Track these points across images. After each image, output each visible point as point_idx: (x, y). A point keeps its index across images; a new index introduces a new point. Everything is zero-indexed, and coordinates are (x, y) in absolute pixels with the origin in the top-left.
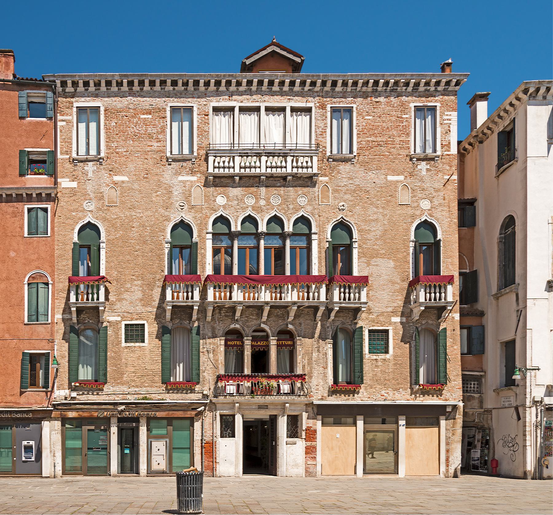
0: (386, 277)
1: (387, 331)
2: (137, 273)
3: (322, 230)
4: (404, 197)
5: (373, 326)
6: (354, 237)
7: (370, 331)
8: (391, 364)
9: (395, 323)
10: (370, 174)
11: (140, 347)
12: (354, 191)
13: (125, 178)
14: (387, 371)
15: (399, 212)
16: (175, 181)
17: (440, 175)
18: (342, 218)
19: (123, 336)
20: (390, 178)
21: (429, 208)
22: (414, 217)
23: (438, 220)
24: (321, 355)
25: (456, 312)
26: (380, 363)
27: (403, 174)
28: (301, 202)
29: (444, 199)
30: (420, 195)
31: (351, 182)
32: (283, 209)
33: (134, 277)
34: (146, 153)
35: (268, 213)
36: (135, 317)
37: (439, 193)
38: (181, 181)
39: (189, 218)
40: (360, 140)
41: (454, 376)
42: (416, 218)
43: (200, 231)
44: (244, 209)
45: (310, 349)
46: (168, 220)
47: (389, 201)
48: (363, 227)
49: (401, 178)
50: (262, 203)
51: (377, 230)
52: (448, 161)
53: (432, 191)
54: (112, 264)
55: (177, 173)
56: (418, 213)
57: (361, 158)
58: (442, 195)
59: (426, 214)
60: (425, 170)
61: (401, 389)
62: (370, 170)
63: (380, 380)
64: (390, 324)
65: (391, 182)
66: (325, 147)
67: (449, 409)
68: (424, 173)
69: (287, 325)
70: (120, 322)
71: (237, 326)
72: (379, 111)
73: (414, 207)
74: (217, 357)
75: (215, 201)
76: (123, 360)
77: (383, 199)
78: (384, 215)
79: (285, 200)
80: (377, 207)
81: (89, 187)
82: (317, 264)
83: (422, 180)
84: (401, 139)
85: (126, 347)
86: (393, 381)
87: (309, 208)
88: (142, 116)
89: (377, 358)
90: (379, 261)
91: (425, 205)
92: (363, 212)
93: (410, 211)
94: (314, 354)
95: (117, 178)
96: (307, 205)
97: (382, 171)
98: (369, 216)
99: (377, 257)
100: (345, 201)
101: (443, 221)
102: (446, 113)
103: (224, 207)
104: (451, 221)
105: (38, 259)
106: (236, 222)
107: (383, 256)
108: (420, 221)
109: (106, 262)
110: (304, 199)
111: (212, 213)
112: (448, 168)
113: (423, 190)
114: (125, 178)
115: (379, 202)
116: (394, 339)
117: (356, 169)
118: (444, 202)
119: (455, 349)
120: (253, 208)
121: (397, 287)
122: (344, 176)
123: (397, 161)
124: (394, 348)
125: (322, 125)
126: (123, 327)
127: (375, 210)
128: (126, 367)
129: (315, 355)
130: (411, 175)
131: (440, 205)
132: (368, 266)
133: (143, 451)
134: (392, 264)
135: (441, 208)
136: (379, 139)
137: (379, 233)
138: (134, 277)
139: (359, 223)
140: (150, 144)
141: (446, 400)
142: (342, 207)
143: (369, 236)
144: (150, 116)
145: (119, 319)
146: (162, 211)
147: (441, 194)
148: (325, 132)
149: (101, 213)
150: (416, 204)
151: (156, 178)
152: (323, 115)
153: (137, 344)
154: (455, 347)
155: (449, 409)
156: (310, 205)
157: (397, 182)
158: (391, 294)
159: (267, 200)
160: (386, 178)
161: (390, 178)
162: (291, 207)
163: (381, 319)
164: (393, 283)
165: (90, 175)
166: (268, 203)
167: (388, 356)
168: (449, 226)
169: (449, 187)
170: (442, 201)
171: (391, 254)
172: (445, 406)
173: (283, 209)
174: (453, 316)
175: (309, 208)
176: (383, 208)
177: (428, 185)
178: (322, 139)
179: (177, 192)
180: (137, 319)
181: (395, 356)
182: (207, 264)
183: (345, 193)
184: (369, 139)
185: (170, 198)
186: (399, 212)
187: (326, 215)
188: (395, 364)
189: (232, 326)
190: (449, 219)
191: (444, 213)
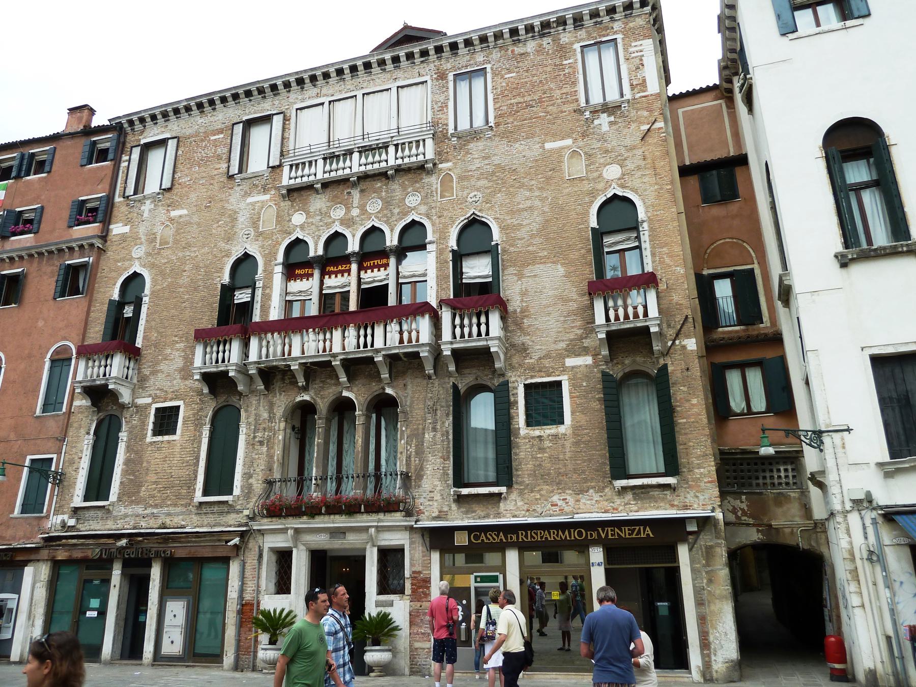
0: (550, 293)
1: (559, 384)
2: (181, 333)
3: (443, 236)
4: (578, 168)
5: (532, 377)
6: (494, 238)
7: (527, 387)
8: (568, 444)
9: (573, 367)
10: (517, 146)
11: (169, 442)
12: (493, 173)
13: (184, 212)
14: (561, 457)
15: (567, 190)
16: (242, 205)
17: (633, 126)
18: (474, 213)
19: (151, 426)
20: (548, 146)
21: (618, 175)
22: (593, 194)
23: (635, 191)
24: (439, 435)
25: (688, 337)
26: (547, 444)
27: (569, 137)
28: (413, 203)
29: (644, 159)
30: (602, 161)
31: (487, 162)
32: (385, 216)
33: (176, 339)
34: (212, 177)
35: (362, 225)
36: (170, 396)
37: (635, 152)
38: (248, 204)
39: (253, 250)
40: (498, 106)
41: (698, 458)
42: (598, 195)
43: (267, 263)
44: (328, 225)
45: (421, 427)
46: (228, 255)
47: (548, 179)
48: (509, 222)
49: (569, 142)
50: (355, 212)
51: (531, 223)
52: (645, 105)
53: (623, 151)
54: (153, 323)
55: (247, 194)
56: (600, 186)
57: (502, 128)
58: (641, 153)
59: (614, 185)
60: (607, 124)
61: (591, 491)
62: (516, 140)
63: (549, 474)
64: (564, 370)
65: (551, 151)
66: (447, 125)
67: (692, 528)
68: (605, 128)
69: (384, 389)
70: (150, 405)
71: (307, 398)
72: (527, 63)
73: (594, 179)
74: (272, 451)
75: (290, 220)
76: (145, 464)
77: (540, 176)
78: (543, 200)
79: (387, 203)
80: (531, 190)
81: (142, 230)
82: (435, 287)
83: (603, 138)
84: (564, 91)
85: (151, 443)
86: (575, 476)
87: (423, 209)
88: (212, 138)
89: (542, 434)
90: (538, 269)
91: (613, 172)
92: (508, 201)
93: (586, 186)
94: (426, 436)
95: (174, 214)
96: (420, 204)
97: (537, 139)
98: (519, 203)
99: (534, 263)
100: (478, 190)
101: (645, 190)
102: (633, 44)
103: (302, 227)
104: (661, 189)
105: (67, 326)
106: (316, 245)
107: (543, 261)
108: (605, 198)
109: (147, 321)
110: (416, 198)
111: (285, 238)
112: (646, 114)
113: (607, 151)
114: (184, 212)
115: (533, 182)
116: (571, 397)
117: (494, 143)
118: (644, 163)
119: (693, 405)
120: (343, 222)
121: (573, 306)
122: (476, 156)
123: (559, 121)
124: (573, 413)
125: (442, 98)
126: (153, 412)
127: (528, 194)
128: (147, 474)
129: (428, 436)
130: (584, 135)
131: (639, 168)
132: (519, 279)
133: (151, 618)
134: (561, 270)
135: (640, 173)
136: (528, 98)
137: (535, 227)
138: (176, 339)
139: (502, 217)
140: (218, 166)
141: (686, 507)
142: (474, 199)
143: (519, 234)
144: (222, 136)
145: (149, 400)
146: (222, 244)
147: (639, 152)
148: (447, 106)
149: (150, 258)
150: (596, 174)
151: (219, 205)
152: (444, 87)
153: (166, 438)
154: (694, 401)
155: (692, 528)
156: (425, 204)
157: (563, 148)
158: (562, 319)
159: (363, 208)
160: (543, 147)
161: (548, 146)
162: (396, 211)
163: (547, 363)
164: (566, 300)
165: (146, 215)
166: (363, 210)
167: (562, 429)
168: (659, 197)
169: (652, 140)
170: (642, 163)
171: (558, 254)
172: (682, 521)
173: (385, 216)
174: (683, 343)
175: (423, 209)
176: (539, 189)
177: (614, 143)
178: (441, 116)
179: (243, 219)
180: (171, 400)
181: (576, 428)
182: (272, 308)
183: (479, 179)
184: (512, 101)
185: (233, 226)
186: (567, 190)
187: (450, 214)
188: (576, 444)
189: (299, 399)
190: (656, 187)
191: (646, 179)
